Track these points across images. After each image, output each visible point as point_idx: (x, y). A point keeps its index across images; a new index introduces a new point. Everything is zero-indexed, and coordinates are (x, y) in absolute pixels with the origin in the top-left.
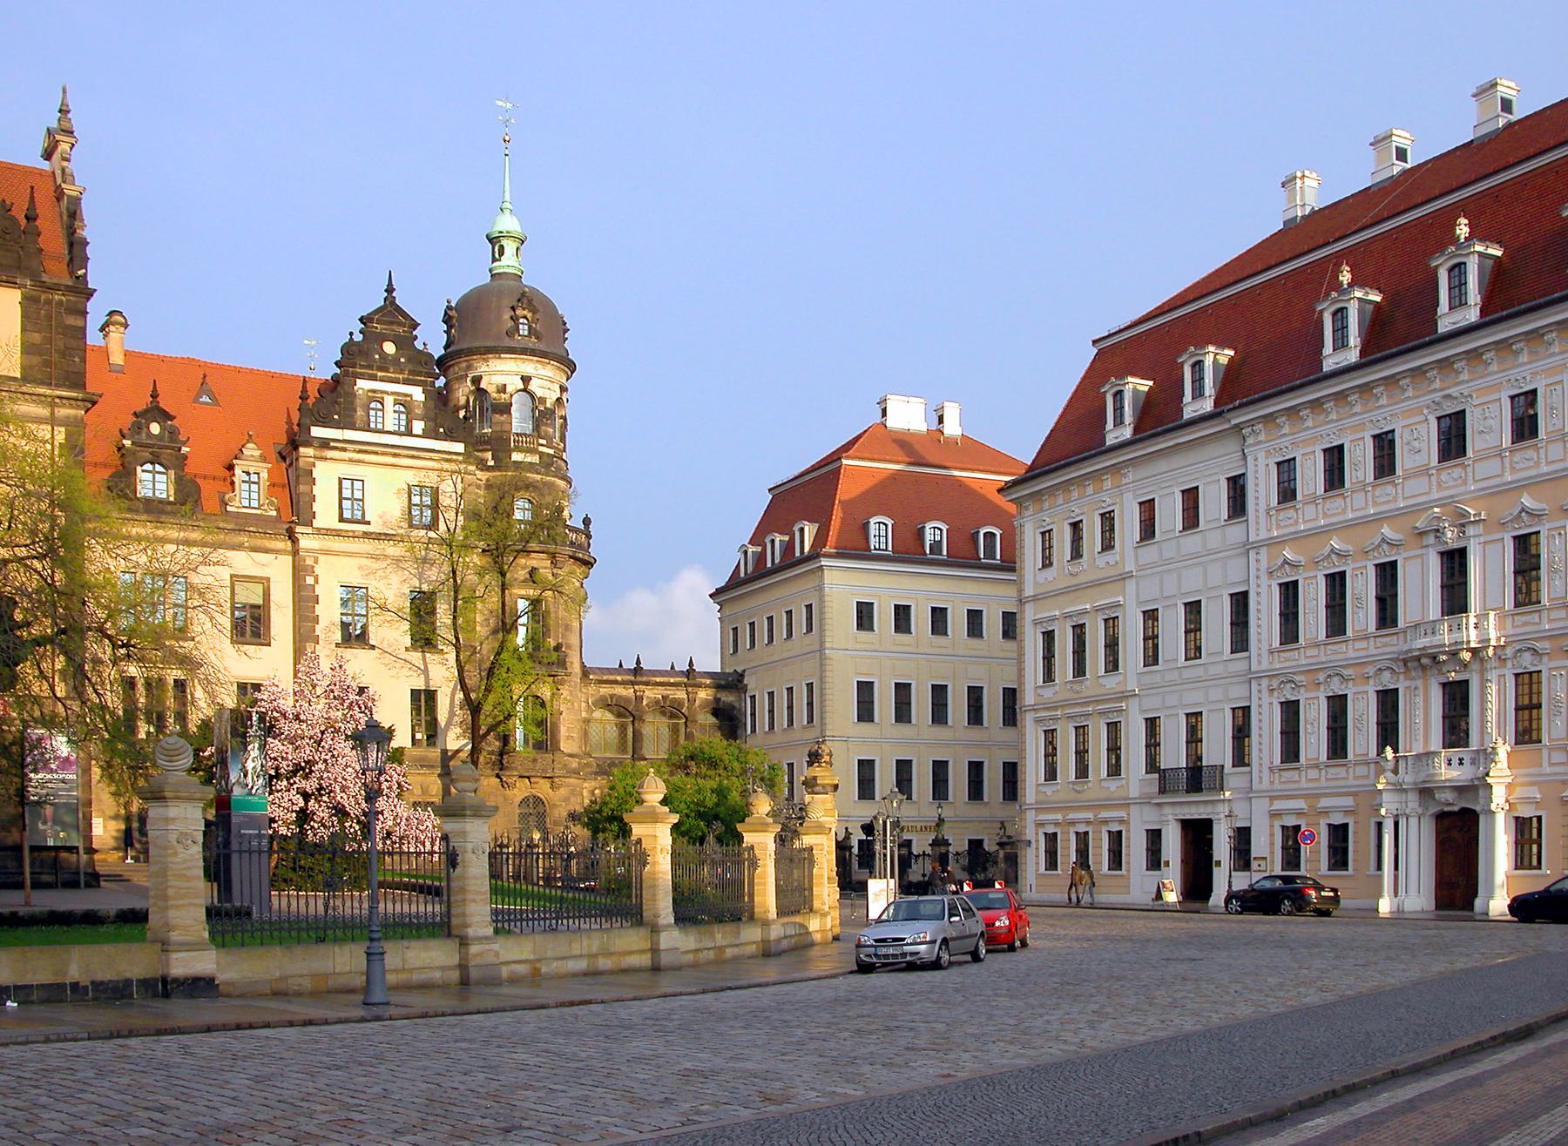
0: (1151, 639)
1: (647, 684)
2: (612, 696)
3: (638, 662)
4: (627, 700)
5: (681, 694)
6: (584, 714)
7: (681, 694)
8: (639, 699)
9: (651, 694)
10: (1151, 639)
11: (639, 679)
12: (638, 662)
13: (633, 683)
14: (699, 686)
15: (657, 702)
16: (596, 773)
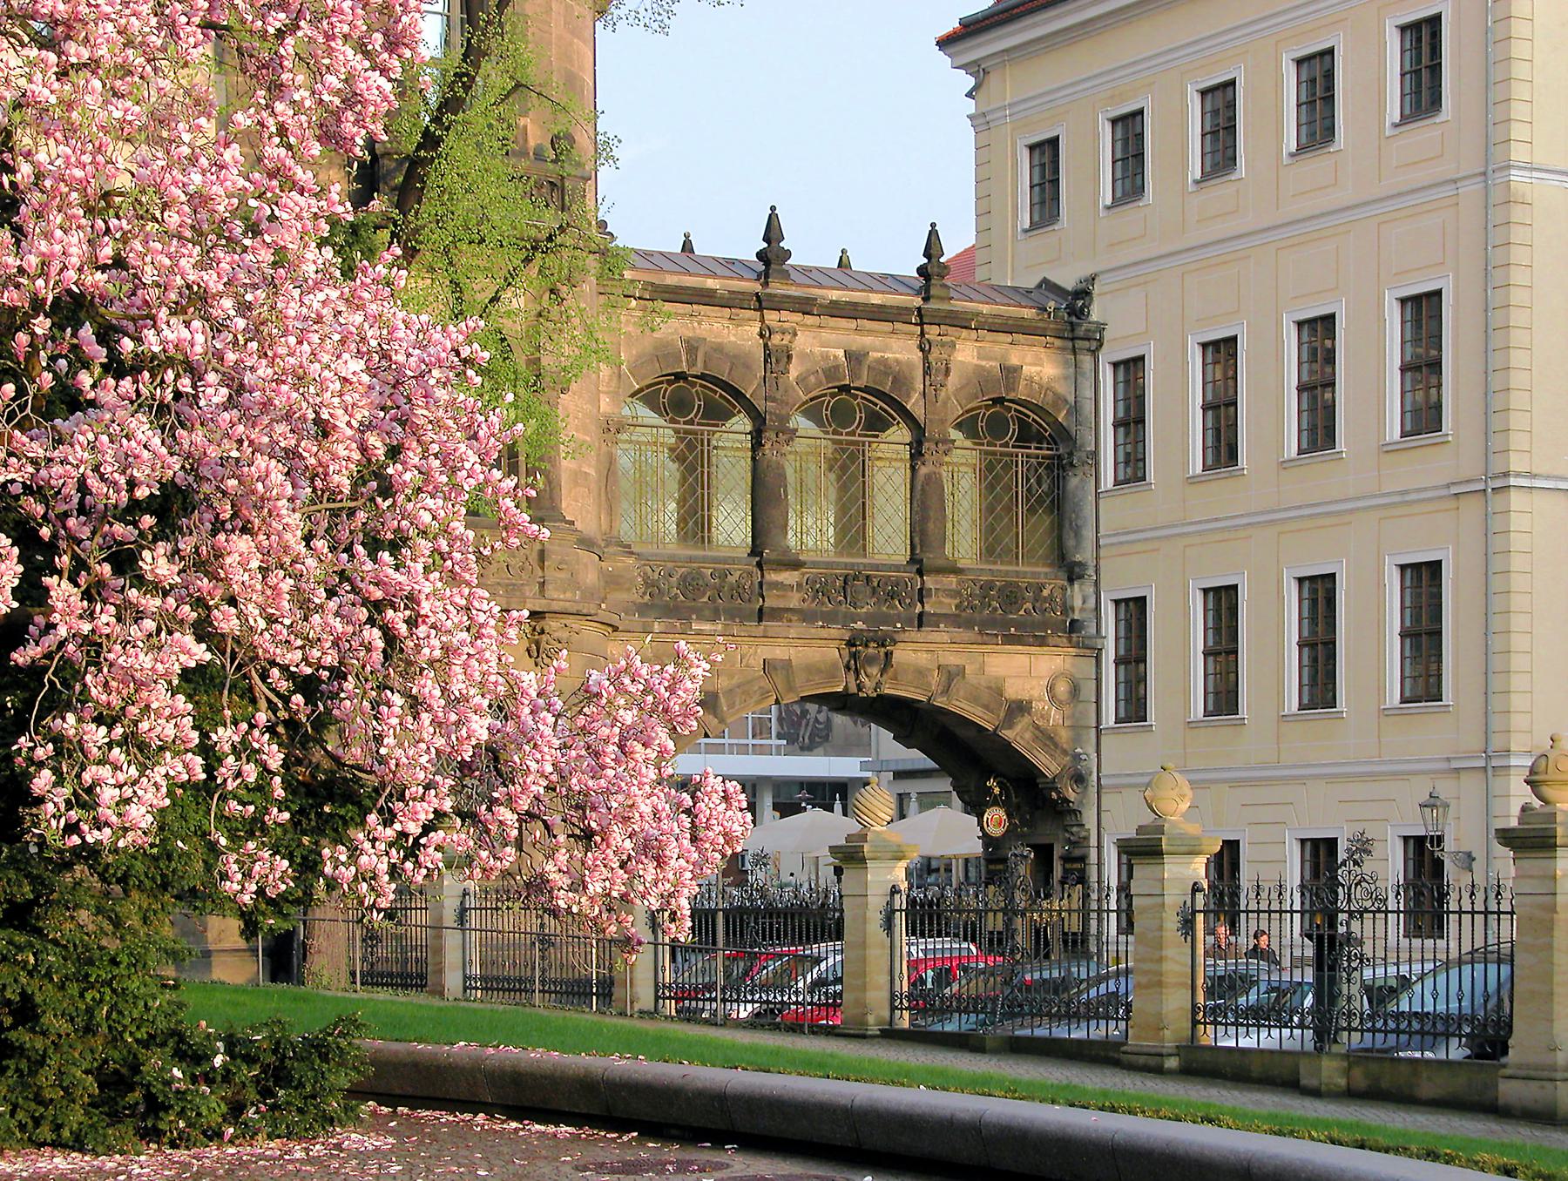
0: (1221, 410)
1: (805, 306)
2: (692, 347)
3: (773, 232)
4: (738, 360)
5: (900, 349)
6: (605, 404)
7: (900, 349)
8: (777, 358)
9: (818, 345)
10: (1221, 410)
11: (777, 288)
12: (773, 232)
13: (761, 303)
14: (960, 321)
15: (831, 372)
16: (643, 609)
